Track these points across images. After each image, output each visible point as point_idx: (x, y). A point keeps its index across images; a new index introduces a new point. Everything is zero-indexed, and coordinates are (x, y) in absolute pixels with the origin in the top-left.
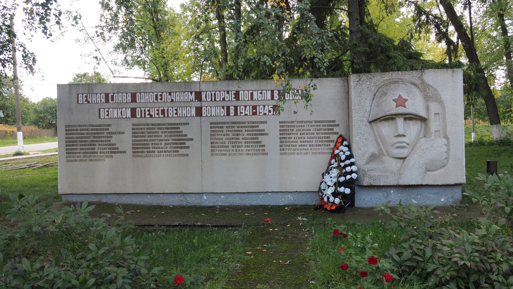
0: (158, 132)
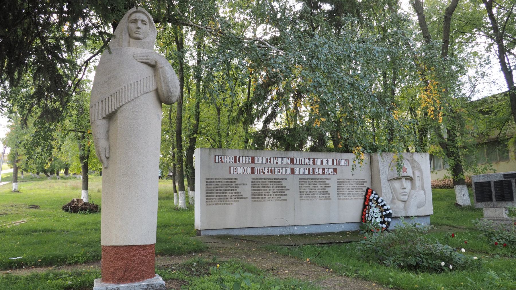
0: (268, 184)
